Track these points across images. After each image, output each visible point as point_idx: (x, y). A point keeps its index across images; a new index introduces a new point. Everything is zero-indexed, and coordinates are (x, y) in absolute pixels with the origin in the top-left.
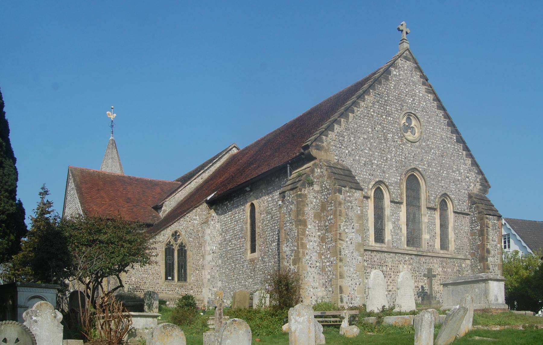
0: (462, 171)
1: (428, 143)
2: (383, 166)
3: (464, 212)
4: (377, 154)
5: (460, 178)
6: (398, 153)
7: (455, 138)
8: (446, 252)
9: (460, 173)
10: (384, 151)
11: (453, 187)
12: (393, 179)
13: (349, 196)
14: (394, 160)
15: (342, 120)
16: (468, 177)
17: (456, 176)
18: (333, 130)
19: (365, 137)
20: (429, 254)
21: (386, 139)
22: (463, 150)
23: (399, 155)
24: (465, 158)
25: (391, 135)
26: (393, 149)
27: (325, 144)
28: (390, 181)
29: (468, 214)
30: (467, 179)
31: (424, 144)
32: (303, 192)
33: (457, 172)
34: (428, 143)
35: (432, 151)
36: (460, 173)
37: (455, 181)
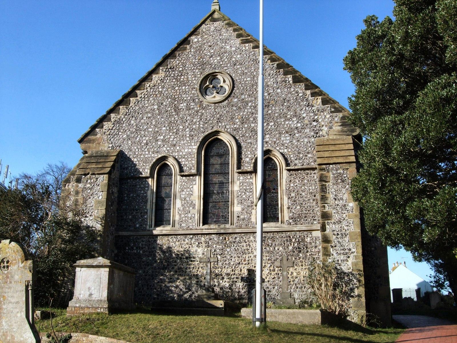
0: (304, 115)
1: (243, 97)
2: (171, 139)
3: (309, 167)
4: (164, 128)
5: (299, 125)
6: (195, 120)
7: (290, 79)
8: (272, 224)
9: (301, 119)
10: (174, 123)
11: (286, 139)
12: (186, 150)
13: (90, 183)
14: (187, 130)
15: (121, 107)
16: (317, 121)
17: (294, 123)
18: (110, 120)
19: (149, 115)
20: (238, 231)
21: (177, 110)
22: (306, 89)
23: (196, 122)
24: (310, 98)
25: (185, 104)
26: (188, 118)
27: (99, 136)
28: (181, 153)
29: (314, 169)
30: (315, 123)
31: (236, 100)
32: (66, 187)
33: (295, 119)
34: (243, 97)
35: (250, 104)
36: (301, 119)
37: (290, 132)
